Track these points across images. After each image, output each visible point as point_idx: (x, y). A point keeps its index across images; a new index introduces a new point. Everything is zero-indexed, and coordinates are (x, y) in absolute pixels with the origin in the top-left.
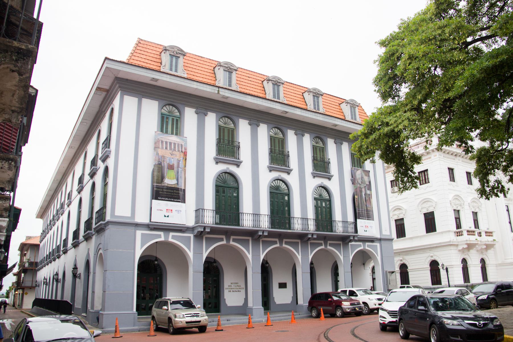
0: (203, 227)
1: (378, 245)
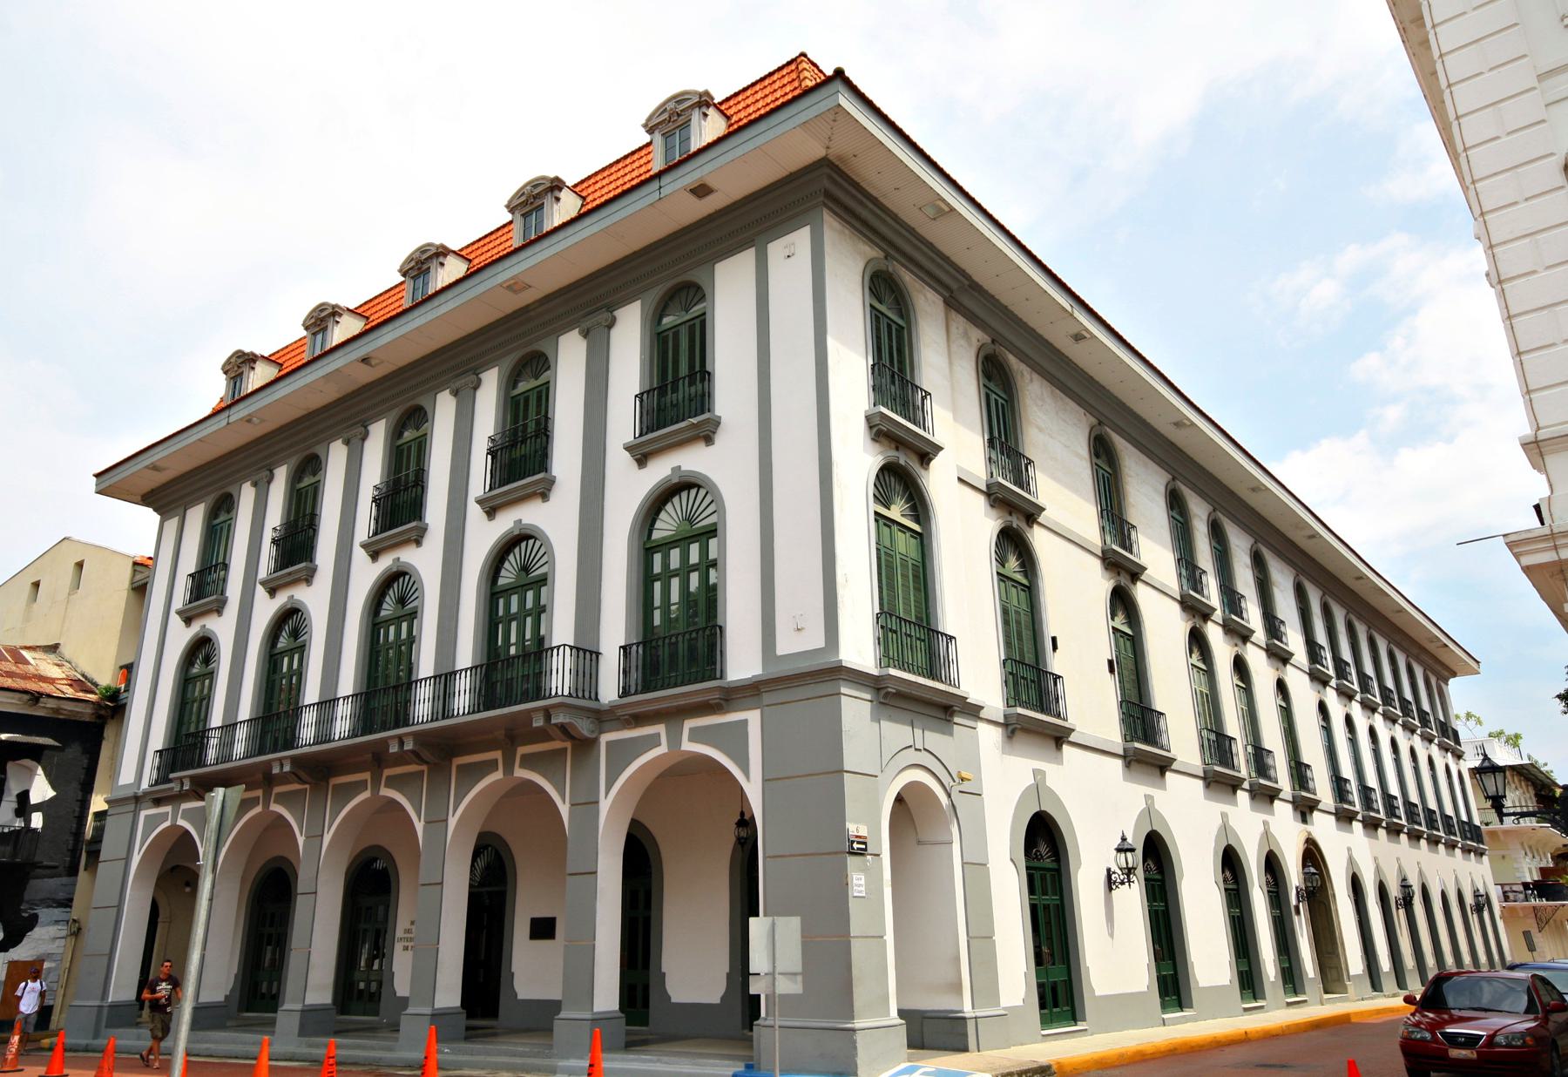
1: (753, 718)
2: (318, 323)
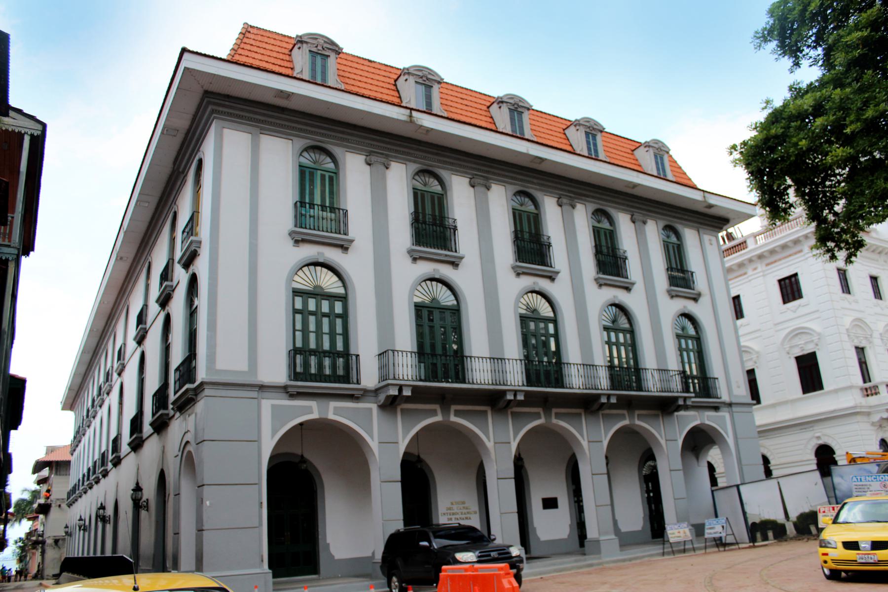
0: (397, 388)
2: (425, 79)
